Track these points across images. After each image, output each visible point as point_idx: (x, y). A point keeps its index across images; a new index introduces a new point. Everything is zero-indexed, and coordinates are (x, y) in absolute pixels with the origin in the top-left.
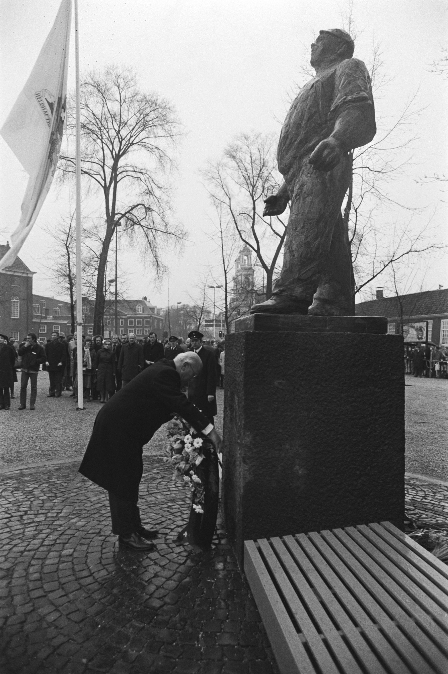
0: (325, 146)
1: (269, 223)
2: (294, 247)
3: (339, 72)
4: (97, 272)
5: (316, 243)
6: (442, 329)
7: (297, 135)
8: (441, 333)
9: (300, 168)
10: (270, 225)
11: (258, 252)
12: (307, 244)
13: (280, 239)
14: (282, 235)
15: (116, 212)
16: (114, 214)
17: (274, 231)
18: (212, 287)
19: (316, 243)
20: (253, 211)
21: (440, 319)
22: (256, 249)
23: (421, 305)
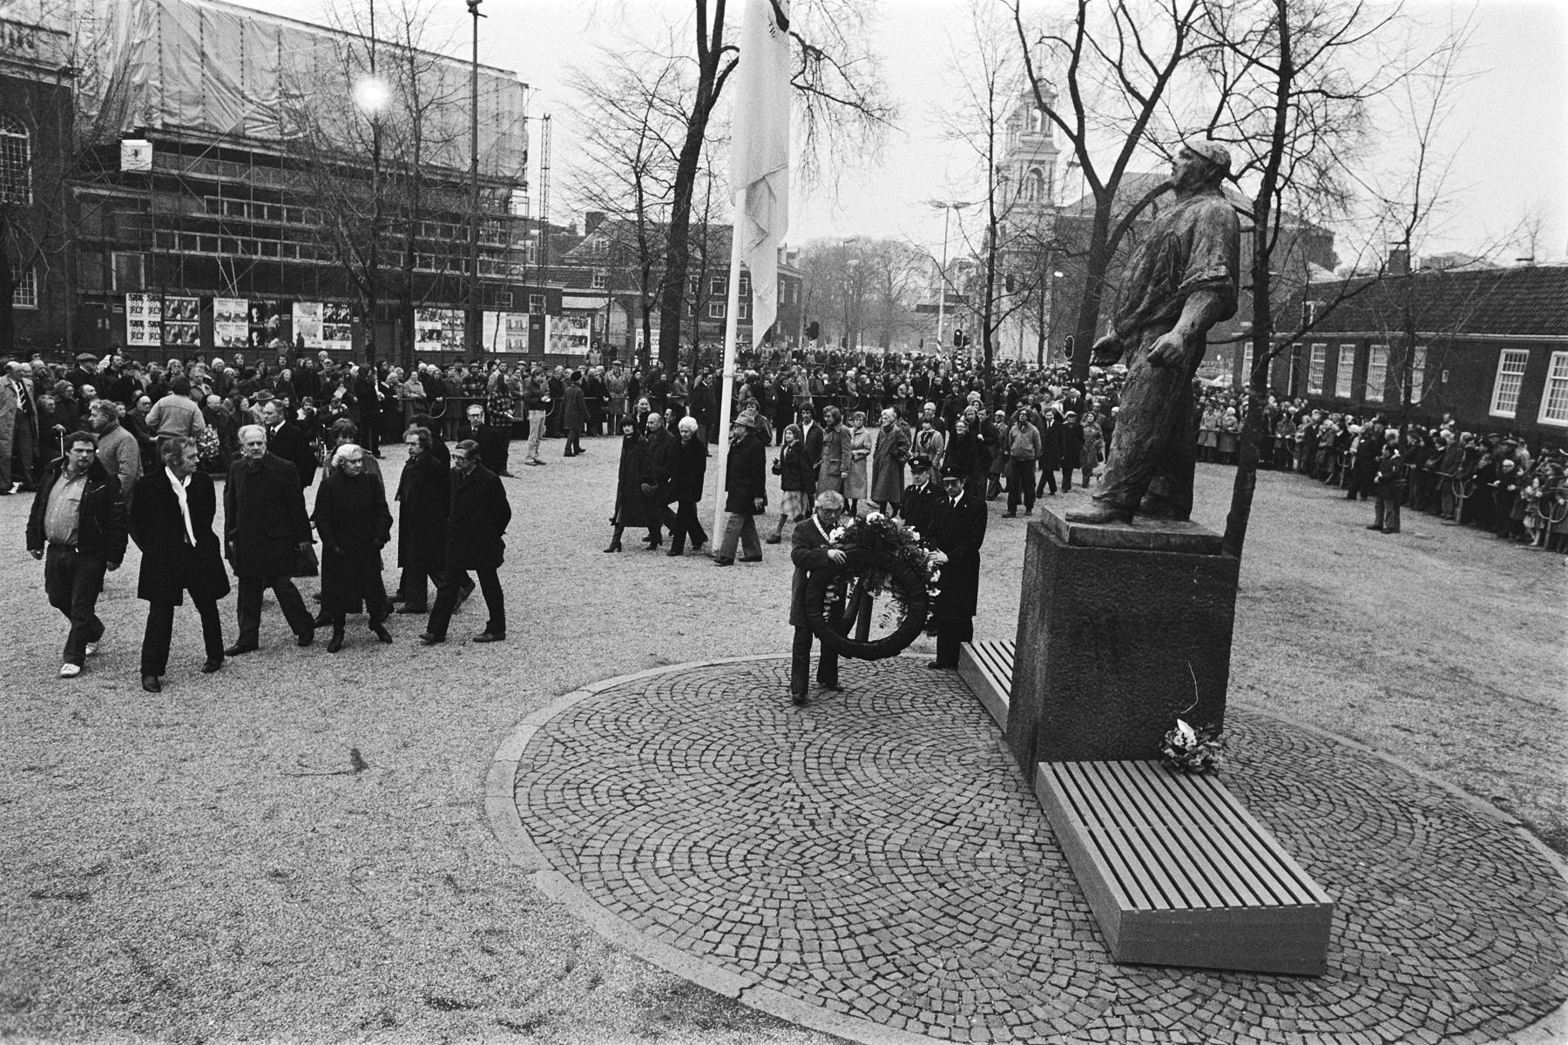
0: (1167, 346)
1: (1116, 59)
2: (1124, 444)
3: (1201, 226)
4: (672, 195)
5: (1149, 441)
6: (1550, 375)
7: (1141, 299)
8: (1548, 387)
9: (1139, 342)
10: (1119, 67)
11: (1079, 140)
12: (1138, 444)
13: (1139, 109)
14: (1147, 96)
15: (724, 43)
16: (718, 50)
17: (1127, 84)
18: (940, 205)
19: (1149, 441)
20: (1076, 27)
21: (1549, 347)
22: (1075, 133)
23: (1506, 305)
